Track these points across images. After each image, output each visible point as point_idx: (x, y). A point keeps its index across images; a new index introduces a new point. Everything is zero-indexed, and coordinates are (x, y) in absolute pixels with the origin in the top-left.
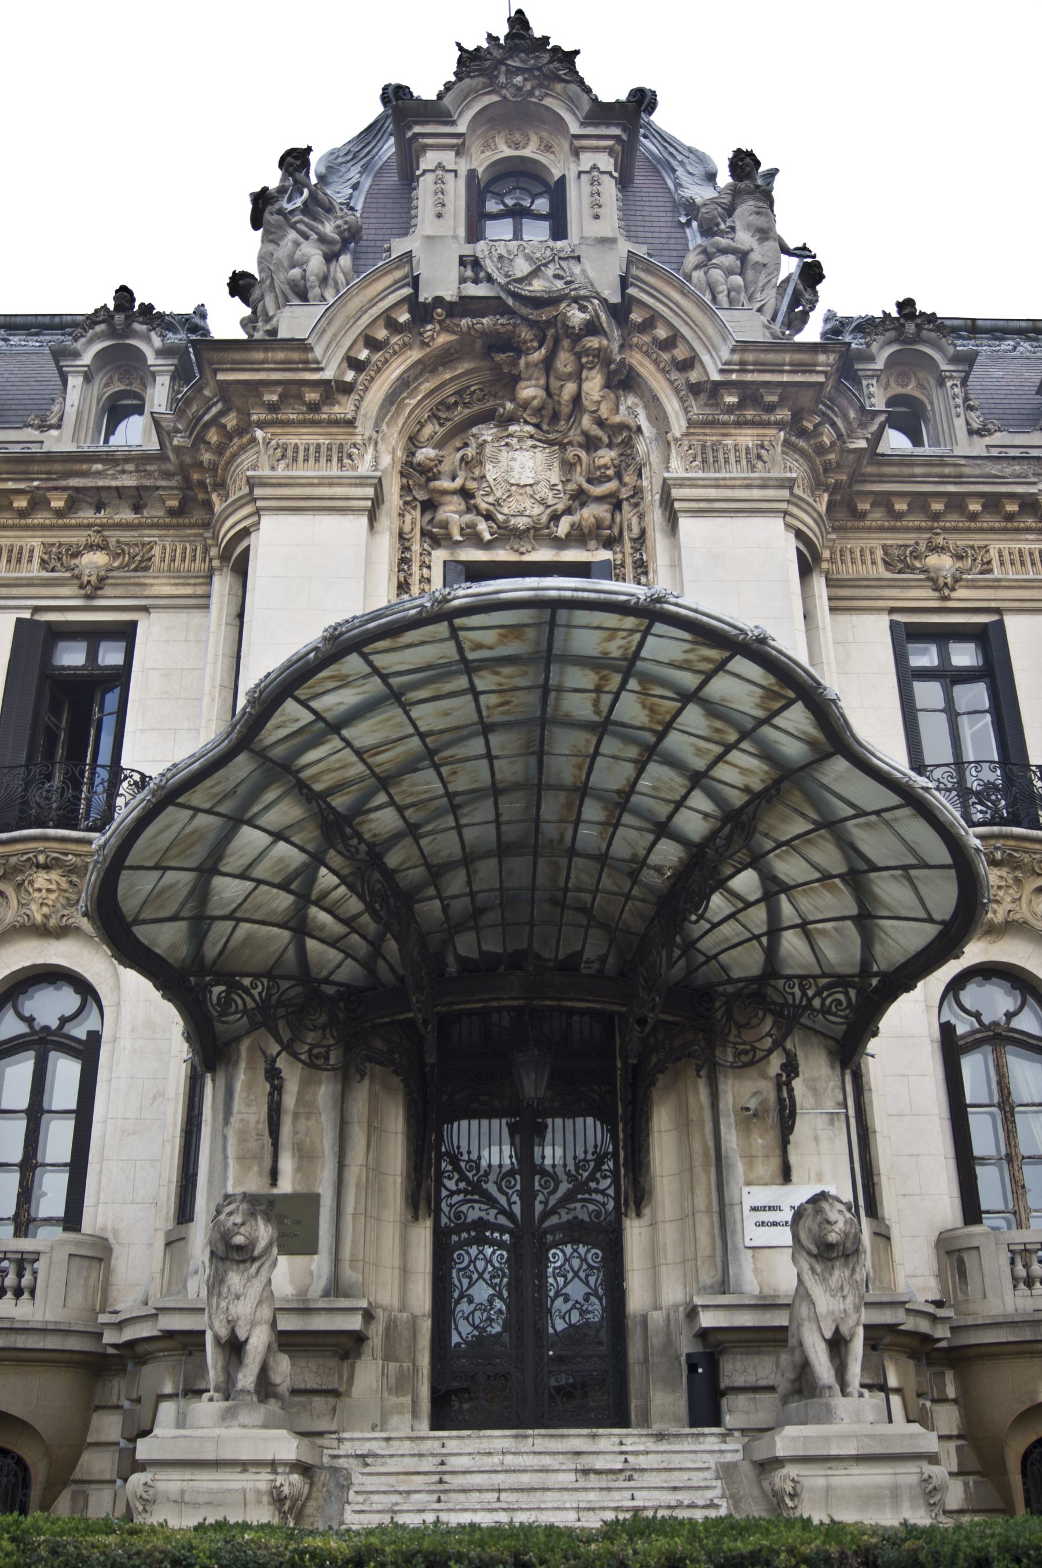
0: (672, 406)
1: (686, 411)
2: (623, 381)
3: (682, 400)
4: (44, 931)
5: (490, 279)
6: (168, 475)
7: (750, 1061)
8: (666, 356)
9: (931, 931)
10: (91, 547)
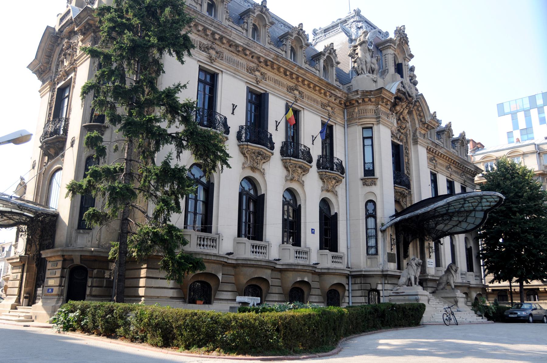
0: (417, 122)
1: (419, 125)
2: (410, 113)
3: (419, 123)
4: (328, 191)
5: (404, 87)
6: (345, 97)
7: (427, 241)
8: (418, 112)
9: (464, 230)
10: (330, 106)
